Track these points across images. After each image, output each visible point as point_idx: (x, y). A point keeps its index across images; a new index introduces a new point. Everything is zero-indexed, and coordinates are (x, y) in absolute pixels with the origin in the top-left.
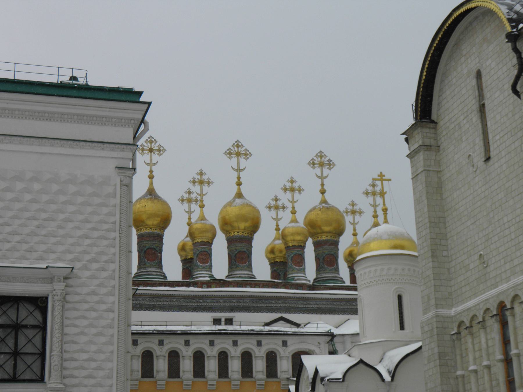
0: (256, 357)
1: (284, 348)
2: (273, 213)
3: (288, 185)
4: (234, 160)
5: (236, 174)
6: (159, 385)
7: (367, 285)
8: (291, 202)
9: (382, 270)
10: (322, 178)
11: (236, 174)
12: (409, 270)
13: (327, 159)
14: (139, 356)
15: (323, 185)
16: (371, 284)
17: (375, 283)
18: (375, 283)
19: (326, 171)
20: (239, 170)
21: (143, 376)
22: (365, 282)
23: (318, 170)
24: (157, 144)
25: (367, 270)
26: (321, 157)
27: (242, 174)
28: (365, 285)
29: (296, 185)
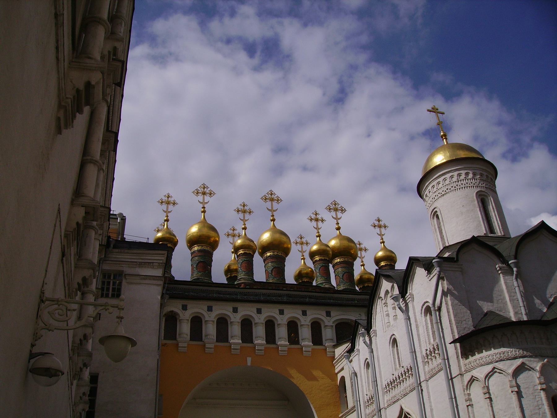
0: (302, 325)
1: (328, 318)
2: (299, 247)
3: (313, 216)
4: (269, 203)
5: (270, 213)
6: (207, 348)
7: (443, 193)
8: (316, 228)
9: (459, 175)
10: (337, 219)
11: (270, 213)
12: (487, 176)
13: (340, 206)
14: (188, 320)
15: (338, 224)
16: (447, 191)
17: (453, 188)
18: (452, 189)
19: (339, 214)
20: (272, 210)
21: (192, 339)
22: (440, 191)
23: (333, 213)
24: (209, 189)
25: (441, 179)
26: (335, 205)
27: (274, 213)
28: (439, 195)
29: (319, 217)
